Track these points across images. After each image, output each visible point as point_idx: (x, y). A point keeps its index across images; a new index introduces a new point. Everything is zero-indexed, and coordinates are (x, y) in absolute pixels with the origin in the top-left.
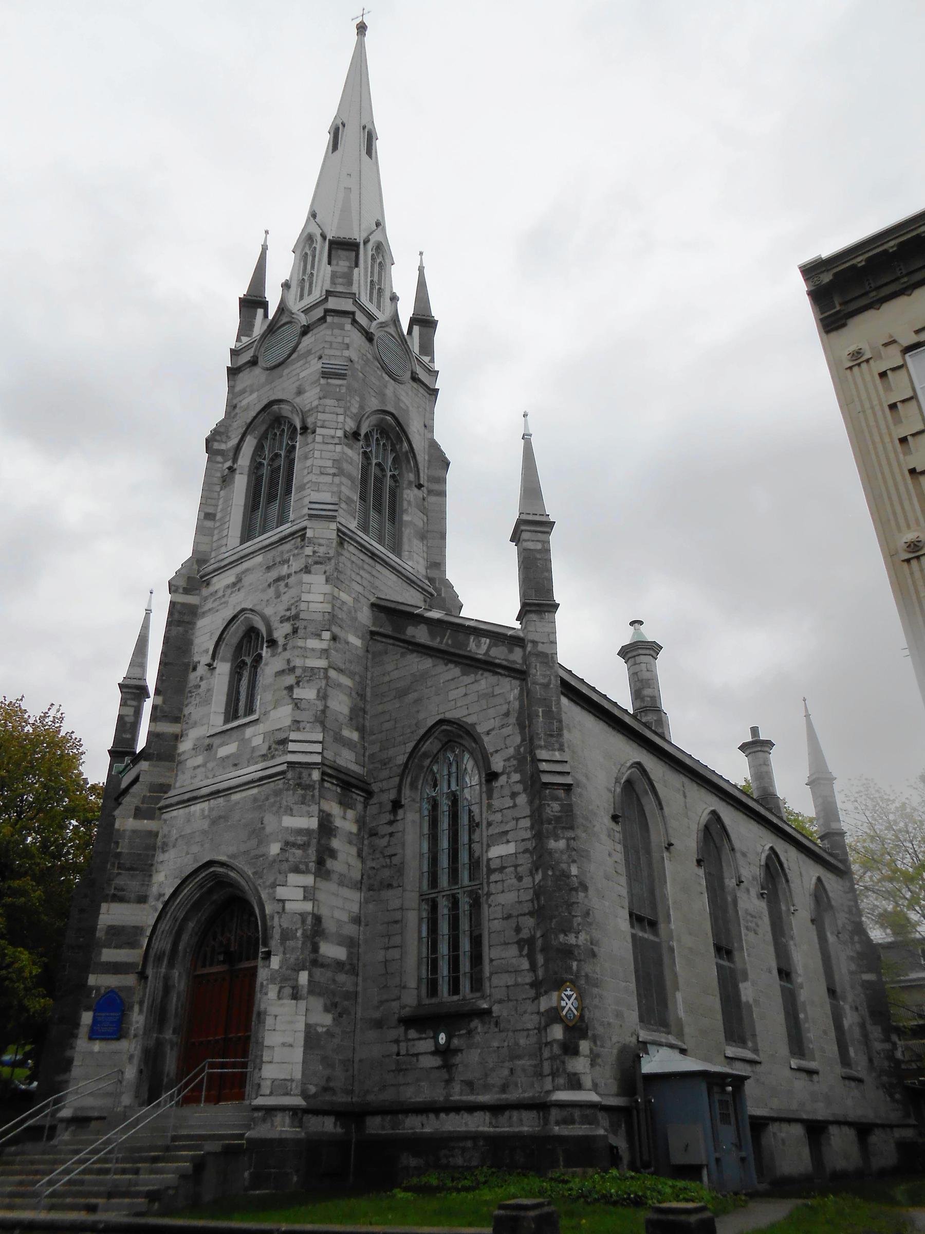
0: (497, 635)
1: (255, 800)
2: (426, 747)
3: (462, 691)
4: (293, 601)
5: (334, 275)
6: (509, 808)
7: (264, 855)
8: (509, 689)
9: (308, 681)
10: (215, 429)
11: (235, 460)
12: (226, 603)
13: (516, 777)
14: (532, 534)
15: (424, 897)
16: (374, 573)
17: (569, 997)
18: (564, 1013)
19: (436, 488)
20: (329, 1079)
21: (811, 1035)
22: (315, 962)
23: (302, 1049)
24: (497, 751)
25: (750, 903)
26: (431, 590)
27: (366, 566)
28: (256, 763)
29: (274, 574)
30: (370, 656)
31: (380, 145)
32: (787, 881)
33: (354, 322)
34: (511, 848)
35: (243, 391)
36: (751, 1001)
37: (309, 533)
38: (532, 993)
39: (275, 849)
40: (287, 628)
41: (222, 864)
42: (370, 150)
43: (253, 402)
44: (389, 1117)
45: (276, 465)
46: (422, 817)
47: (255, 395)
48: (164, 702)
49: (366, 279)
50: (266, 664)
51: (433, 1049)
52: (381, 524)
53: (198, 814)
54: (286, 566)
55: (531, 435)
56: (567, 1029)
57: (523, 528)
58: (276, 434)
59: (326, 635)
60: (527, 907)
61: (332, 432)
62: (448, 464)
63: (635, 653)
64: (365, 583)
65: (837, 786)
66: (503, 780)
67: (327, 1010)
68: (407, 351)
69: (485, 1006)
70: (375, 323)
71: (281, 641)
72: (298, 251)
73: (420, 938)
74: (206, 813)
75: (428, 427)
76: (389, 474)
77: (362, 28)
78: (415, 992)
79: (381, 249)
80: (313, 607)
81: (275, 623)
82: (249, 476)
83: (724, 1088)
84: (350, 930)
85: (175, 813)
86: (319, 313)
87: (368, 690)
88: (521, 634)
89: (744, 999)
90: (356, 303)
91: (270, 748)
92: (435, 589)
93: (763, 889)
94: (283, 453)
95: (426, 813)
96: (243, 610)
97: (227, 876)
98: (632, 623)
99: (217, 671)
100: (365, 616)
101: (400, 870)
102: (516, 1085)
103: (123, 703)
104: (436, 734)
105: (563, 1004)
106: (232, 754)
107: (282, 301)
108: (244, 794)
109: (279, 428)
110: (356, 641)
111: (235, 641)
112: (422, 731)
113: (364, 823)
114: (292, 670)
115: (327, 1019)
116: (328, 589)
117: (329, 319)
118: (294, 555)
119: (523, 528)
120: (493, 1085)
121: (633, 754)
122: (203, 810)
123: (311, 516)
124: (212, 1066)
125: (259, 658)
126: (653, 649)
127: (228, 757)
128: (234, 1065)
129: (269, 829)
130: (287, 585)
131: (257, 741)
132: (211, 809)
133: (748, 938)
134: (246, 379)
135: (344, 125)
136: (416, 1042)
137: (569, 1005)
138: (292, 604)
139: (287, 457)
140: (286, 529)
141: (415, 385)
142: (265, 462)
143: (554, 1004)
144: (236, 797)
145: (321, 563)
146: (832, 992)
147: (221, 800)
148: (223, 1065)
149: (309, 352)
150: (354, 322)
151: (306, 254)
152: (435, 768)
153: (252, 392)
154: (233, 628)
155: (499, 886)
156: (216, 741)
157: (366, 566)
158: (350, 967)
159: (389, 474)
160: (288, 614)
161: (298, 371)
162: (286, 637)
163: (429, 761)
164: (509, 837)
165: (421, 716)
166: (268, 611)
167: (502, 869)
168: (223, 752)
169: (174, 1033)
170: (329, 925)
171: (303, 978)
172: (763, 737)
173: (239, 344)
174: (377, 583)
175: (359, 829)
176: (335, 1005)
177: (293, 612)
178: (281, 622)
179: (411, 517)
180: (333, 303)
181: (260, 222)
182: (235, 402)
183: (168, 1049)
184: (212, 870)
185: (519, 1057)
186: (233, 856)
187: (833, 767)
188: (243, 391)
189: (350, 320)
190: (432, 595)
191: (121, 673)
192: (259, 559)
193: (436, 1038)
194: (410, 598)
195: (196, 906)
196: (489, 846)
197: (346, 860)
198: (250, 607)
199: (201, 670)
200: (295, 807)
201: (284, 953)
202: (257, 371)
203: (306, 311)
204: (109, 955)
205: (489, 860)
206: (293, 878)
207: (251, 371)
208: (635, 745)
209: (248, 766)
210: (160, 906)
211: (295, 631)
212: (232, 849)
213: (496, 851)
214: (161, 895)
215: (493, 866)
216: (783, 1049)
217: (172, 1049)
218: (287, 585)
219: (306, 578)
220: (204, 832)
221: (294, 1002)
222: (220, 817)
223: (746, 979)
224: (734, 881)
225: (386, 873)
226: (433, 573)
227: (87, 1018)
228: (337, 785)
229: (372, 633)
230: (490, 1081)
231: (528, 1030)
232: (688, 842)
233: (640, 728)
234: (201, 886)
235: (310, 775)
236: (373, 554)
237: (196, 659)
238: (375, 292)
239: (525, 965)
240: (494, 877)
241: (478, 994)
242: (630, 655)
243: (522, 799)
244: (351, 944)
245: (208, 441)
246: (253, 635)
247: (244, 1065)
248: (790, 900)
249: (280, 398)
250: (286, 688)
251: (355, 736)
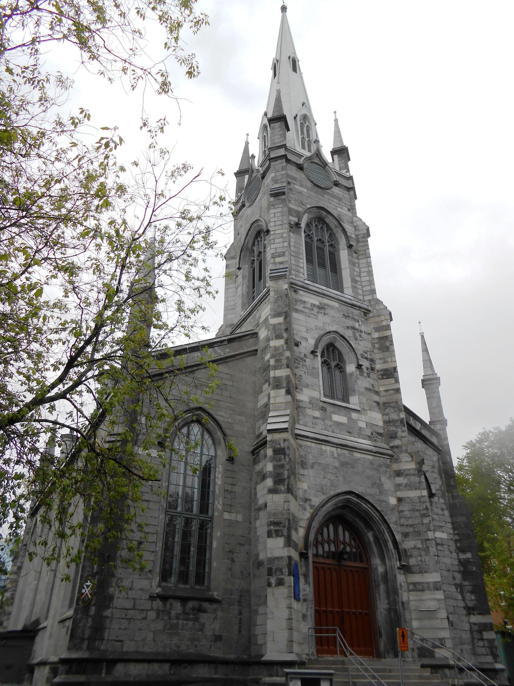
1: (371, 463)
28: (365, 439)
29: (350, 323)
38: (465, 612)
60: (457, 568)
74: (336, 455)
77: (284, 9)
85: (309, 444)
108: (363, 456)
130: (360, 336)
132: (339, 455)
144: (355, 454)
147: (346, 452)
164: (444, 529)
168: (336, 418)
184: (348, 497)
222: (347, 463)
234: (336, 504)
239: (460, 597)
243: (446, 513)
246: (331, 349)
250: (375, 402)
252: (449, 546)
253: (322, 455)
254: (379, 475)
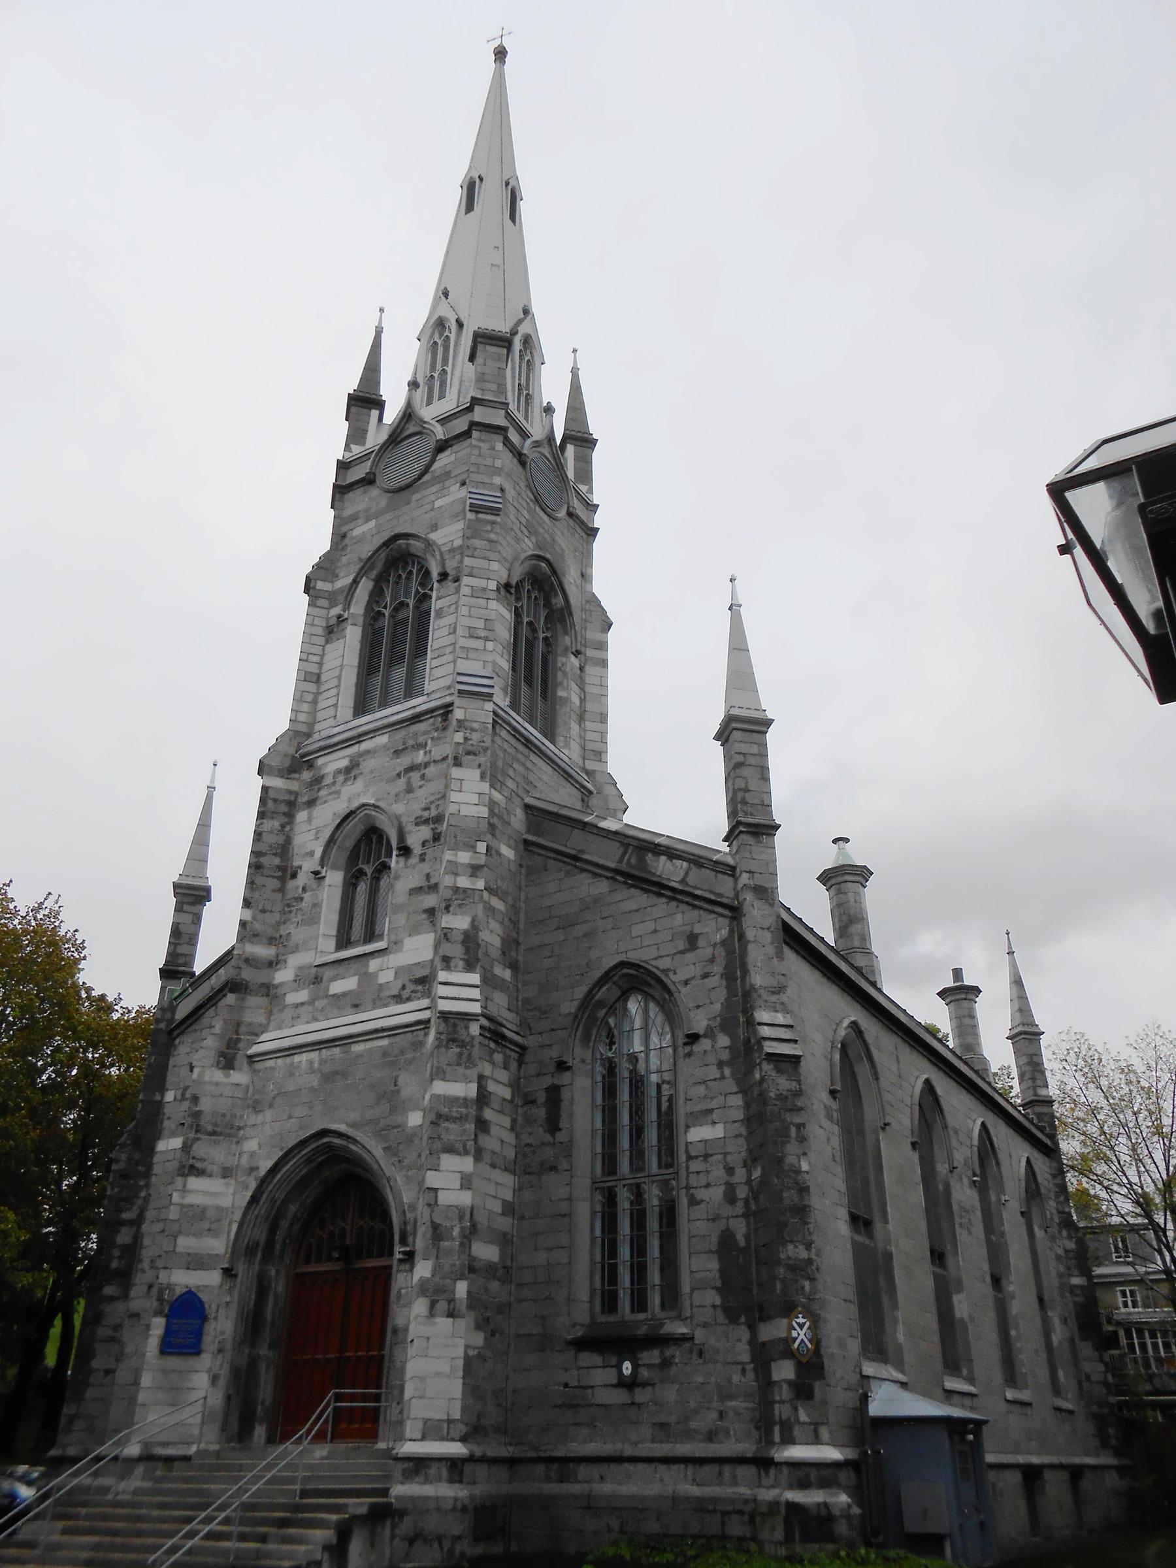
0: (696, 858)
1: (385, 1053)
2: (601, 994)
3: (650, 926)
4: (433, 798)
5: (481, 379)
6: (715, 1080)
7: (399, 1126)
8: (714, 929)
9: (460, 906)
10: (317, 564)
11: (347, 605)
12: (339, 792)
13: (724, 1040)
14: (743, 734)
15: (596, 1185)
16: (529, 764)
17: (801, 1326)
18: (796, 1346)
19: (594, 656)
20: (479, 1417)
21: (1022, 1357)
22: (472, 1269)
23: (460, 1381)
24: (698, 1007)
25: (964, 1195)
26: (589, 786)
27: (519, 756)
28: (386, 1006)
29: (405, 761)
30: (523, 871)
31: (523, 207)
32: (998, 1163)
33: (507, 442)
34: (718, 1132)
35: (354, 517)
36: (966, 1316)
37: (458, 714)
39: (415, 1119)
40: (425, 832)
41: (340, 1135)
42: (513, 216)
43: (369, 535)
44: (555, 1467)
45: (401, 616)
46: (594, 1082)
47: (372, 524)
48: (254, 918)
49: (514, 382)
50: (397, 878)
51: (615, 1381)
52: (532, 701)
53: (304, 1065)
54: (422, 752)
55: (740, 606)
56: (801, 1367)
57: (734, 725)
58: (400, 576)
59: (482, 847)
61: (482, 583)
62: (610, 625)
63: (840, 879)
64: (519, 779)
65: (1044, 1041)
66: (705, 1044)
67: (478, 1327)
68: (564, 478)
69: (685, 1330)
70: (528, 442)
71: (417, 849)
72: (425, 339)
73: (593, 1239)
74: (316, 1065)
75: (585, 577)
76: (542, 636)
77: (501, 54)
78: (587, 1306)
79: (529, 342)
80: (466, 811)
81: (409, 827)
82: (364, 627)
83: (962, 1434)
84: (505, 1224)
85: (271, 1063)
86: (461, 425)
87: (522, 915)
88: (730, 861)
89: (958, 1315)
90: (508, 416)
91: (404, 987)
92: (595, 786)
93: (975, 1175)
94: (411, 602)
95: (599, 1078)
96: (364, 805)
97: (347, 1149)
98: (835, 841)
99: (327, 881)
100: (518, 820)
101: (567, 1150)
102: (728, 1433)
103: (178, 909)
104: (615, 978)
105: (794, 1334)
106: (350, 991)
107: (409, 404)
108: (369, 1045)
109: (404, 568)
110: (508, 852)
111: (350, 844)
112: (597, 974)
113: (518, 1087)
114: (434, 888)
115: (479, 1339)
116: (485, 787)
117: (475, 434)
118: (433, 739)
119: (734, 725)
120: (696, 1431)
121: (852, 1013)
122: (311, 1062)
123: (460, 692)
124: (338, 1397)
125: (385, 867)
126: (862, 874)
127: (345, 995)
128: (364, 1397)
129: (405, 1093)
130: (423, 777)
131: (386, 977)
132: (322, 1062)
133: (962, 1236)
134: (359, 501)
135: (481, 179)
136: (591, 1371)
137: (802, 1336)
138: (431, 803)
139: (416, 607)
140: (419, 703)
141: (571, 522)
142: (387, 613)
143: (784, 1335)
144: (358, 1048)
145: (475, 754)
146: (1041, 1300)
147: (337, 1050)
148: (352, 1397)
149: (447, 475)
150: (507, 442)
151: (435, 343)
152: (611, 1021)
153: (368, 520)
154: (348, 827)
155: (703, 1179)
156: (328, 973)
157: (519, 756)
158: (502, 1272)
159: (542, 636)
160: (426, 814)
161: (432, 497)
162: (424, 844)
163: (604, 1011)
164: (715, 1116)
165: (594, 954)
166: (399, 808)
167: (706, 1156)
169: (269, 1349)
170: (482, 1219)
171: (462, 1289)
172: (968, 981)
173: (348, 455)
174: (531, 778)
175: (513, 1095)
176: (487, 1320)
177: (434, 813)
178: (417, 824)
179: (569, 692)
180: (479, 414)
181: (376, 297)
182: (344, 529)
183: (263, 1368)
184: (325, 1140)
185: (732, 1397)
186: (353, 1125)
187: (1041, 1019)
188: (354, 517)
189: (501, 438)
190: (591, 793)
191: (174, 868)
192: (383, 740)
193: (619, 1367)
194: (563, 797)
195: (302, 1184)
196: (688, 1127)
197: (501, 1134)
198: (372, 802)
199: (303, 878)
200: (449, 1069)
201: (437, 1257)
202: (374, 492)
203: (443, 421)
204: (185, 1243)
205: (687, 1144)
206: (449, 1162)
207: (365, 492)
208: (849, 999)
209: (374, 1008)
210: (253, 1185)
211: (436, 838)
212: (354, 1116)
213: (698, 1134)
214: (253, 1169)
215: (693, 1153)
216: (998, 1377)
217: (268, 1368)
218: (423, 777)
219: (456, 772)
220: (313, 1090)
221: (450, 1320)
222: (336, 1073)
223: (960, 1289)
224: (946, 1166)
225: (549, 1153)
226: (590, 765)
227: (158, 1326)
228: (490, 1039)
229: (526, 841)
230: (693, 1425)
231: (742, 1363)
232: (904, 1120)
233: (844, 971)
234: (309, 1161)
235: (467, 1028)
236: (527, 740)
237: (296, 863)
238: (523, 399)
240: (695, 1166)
241: (673, 1314)
242: (833, 881)
244: (504, 1240)
245: (308, 579)
246: (374, 838)
247: (377, 1398)
248: (1001, 1189)
249: (413, 532)
250: (425, 911)
251: (507, 974)
252: (726, 1154)
253: (292, 1074)
254: (395, 1074)
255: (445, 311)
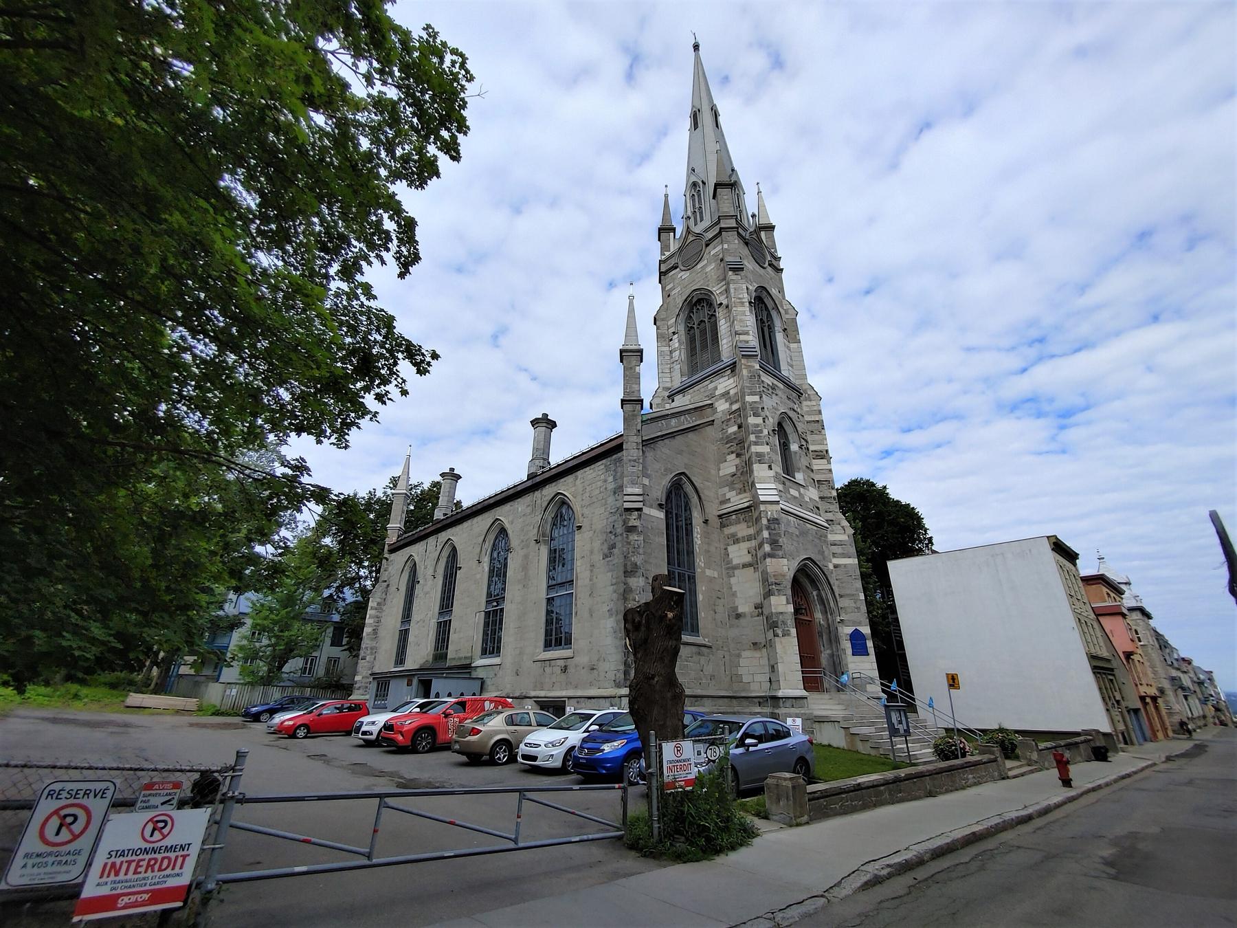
31: (721, 119)
75: (781, 291)
86: (717, 229)
255: (694, 179)
